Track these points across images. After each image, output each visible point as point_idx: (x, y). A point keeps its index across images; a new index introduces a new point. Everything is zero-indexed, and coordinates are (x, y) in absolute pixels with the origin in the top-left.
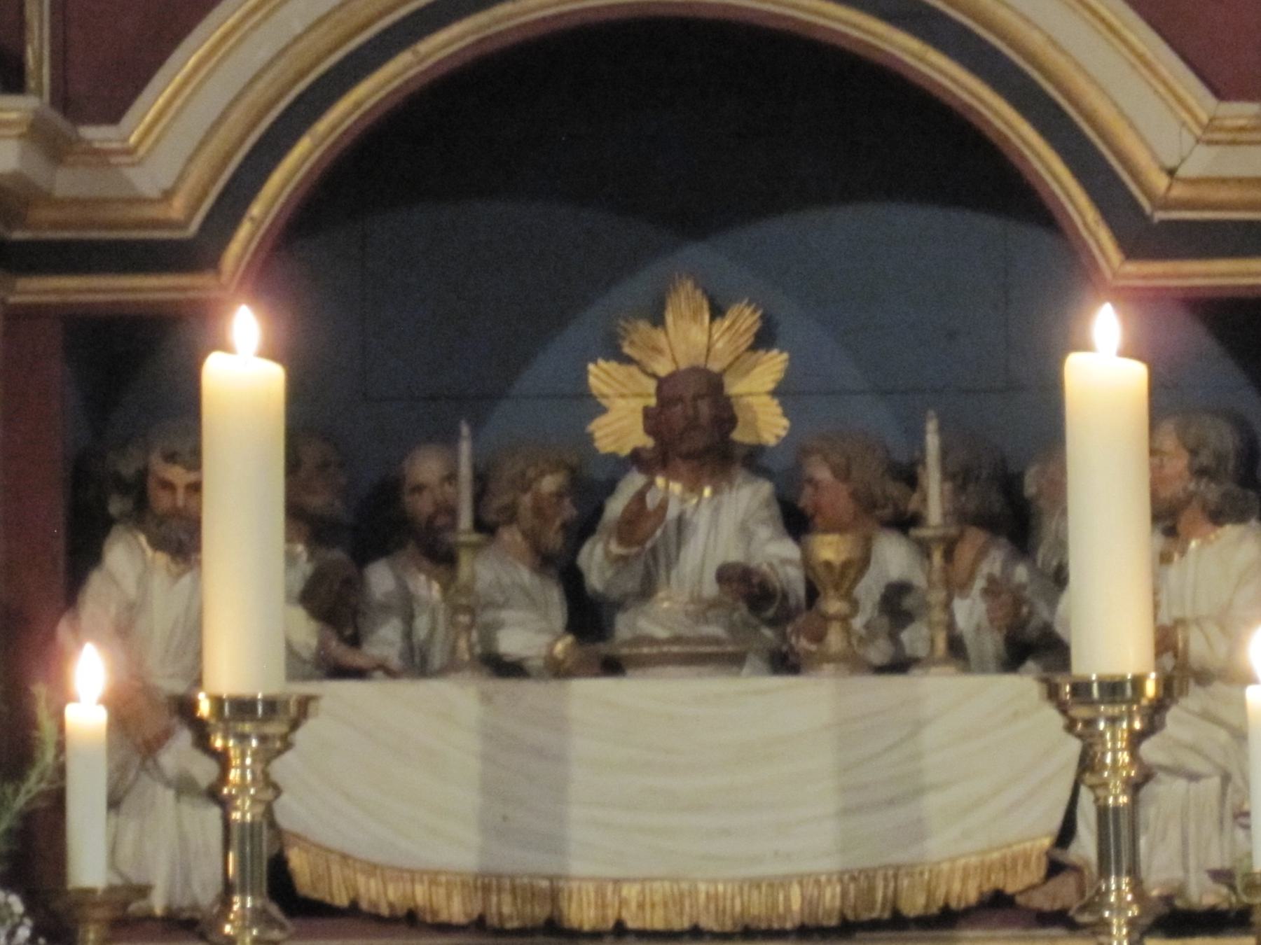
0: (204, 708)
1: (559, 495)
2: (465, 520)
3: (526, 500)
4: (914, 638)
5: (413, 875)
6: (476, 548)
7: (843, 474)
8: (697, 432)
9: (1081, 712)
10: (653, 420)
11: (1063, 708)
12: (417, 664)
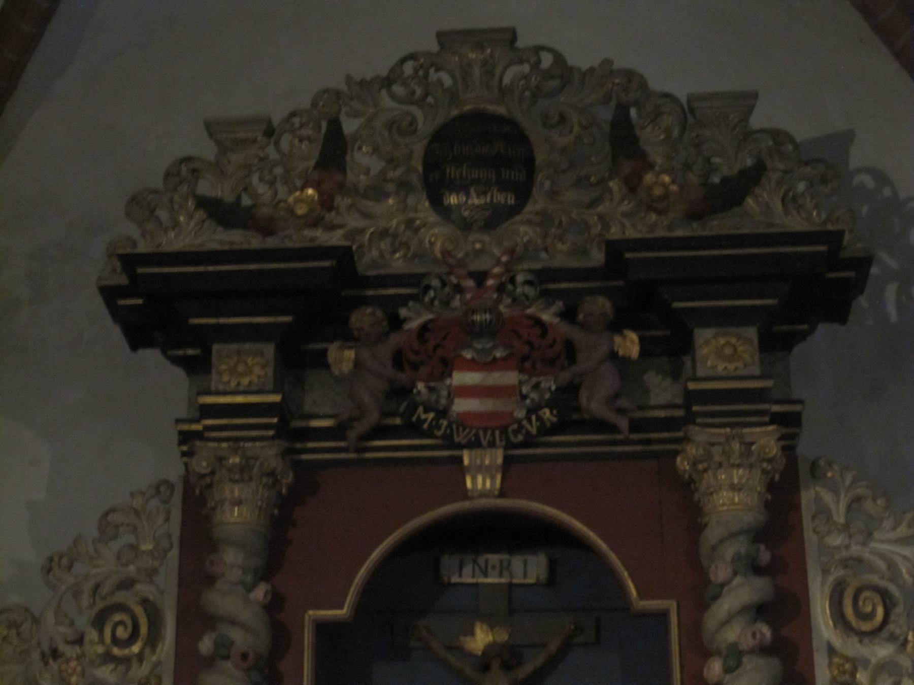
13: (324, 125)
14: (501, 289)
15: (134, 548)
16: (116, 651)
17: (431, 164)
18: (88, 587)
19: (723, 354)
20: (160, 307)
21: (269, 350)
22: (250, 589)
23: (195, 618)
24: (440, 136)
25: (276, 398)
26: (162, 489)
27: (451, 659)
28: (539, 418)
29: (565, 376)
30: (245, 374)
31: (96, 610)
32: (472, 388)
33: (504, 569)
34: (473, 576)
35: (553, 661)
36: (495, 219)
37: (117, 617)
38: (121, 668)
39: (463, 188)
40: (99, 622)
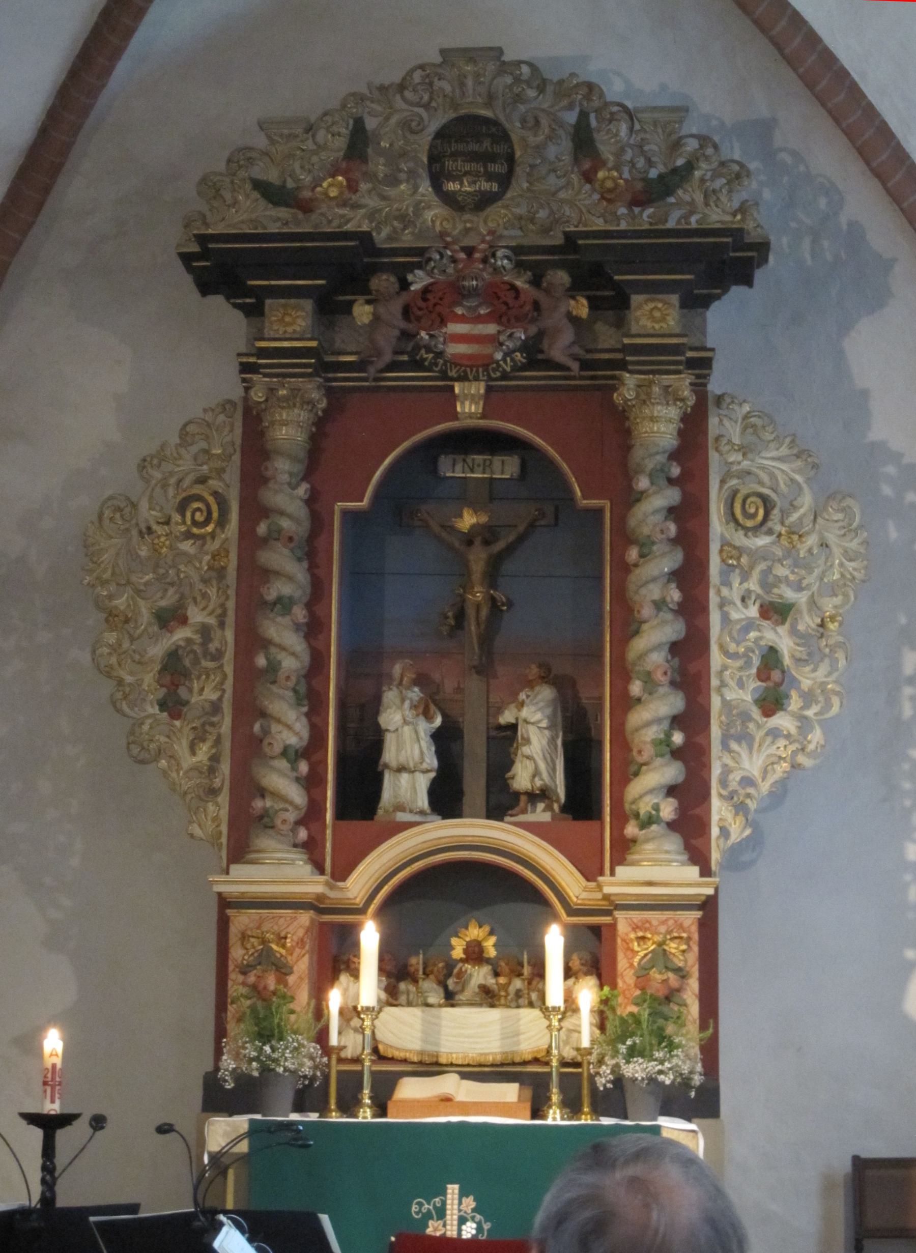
0: (359, 1009)
1: (443, 968)
2: (421, 972)
3: (436, 969)
4: (521, 1001)
5: (406, 1051)
6: (424, 979)
7: (507, 964)
8: (475, 954)
9: (547, 1014)
10: (465, 951)
11: (543, 1013)
12: (409, 1004)
13: (351, 122)
14: (485, 261)
15: (206, 452)
16: (195, 530)
17: (434, 158)
18: (173, 481)
19: (654, 316)
20: (224, 269)
21: (308, 304)
22: (294, 488)
23: (254, 510)
24: (441, 135)
25: (314, 344)
26: (227, 406)
27: (444, 534)
28: (512, 360)
29: (533, 330)
30: (292, 322)
31: (180, 498)
32: (462, 335)
33: (486, 467)
34: (463, 472)
35: (521, 539)
36: (483, 202)
37: (196, 505)
38: (199, 543)
39: (458, 178)
40: (182, 508)
